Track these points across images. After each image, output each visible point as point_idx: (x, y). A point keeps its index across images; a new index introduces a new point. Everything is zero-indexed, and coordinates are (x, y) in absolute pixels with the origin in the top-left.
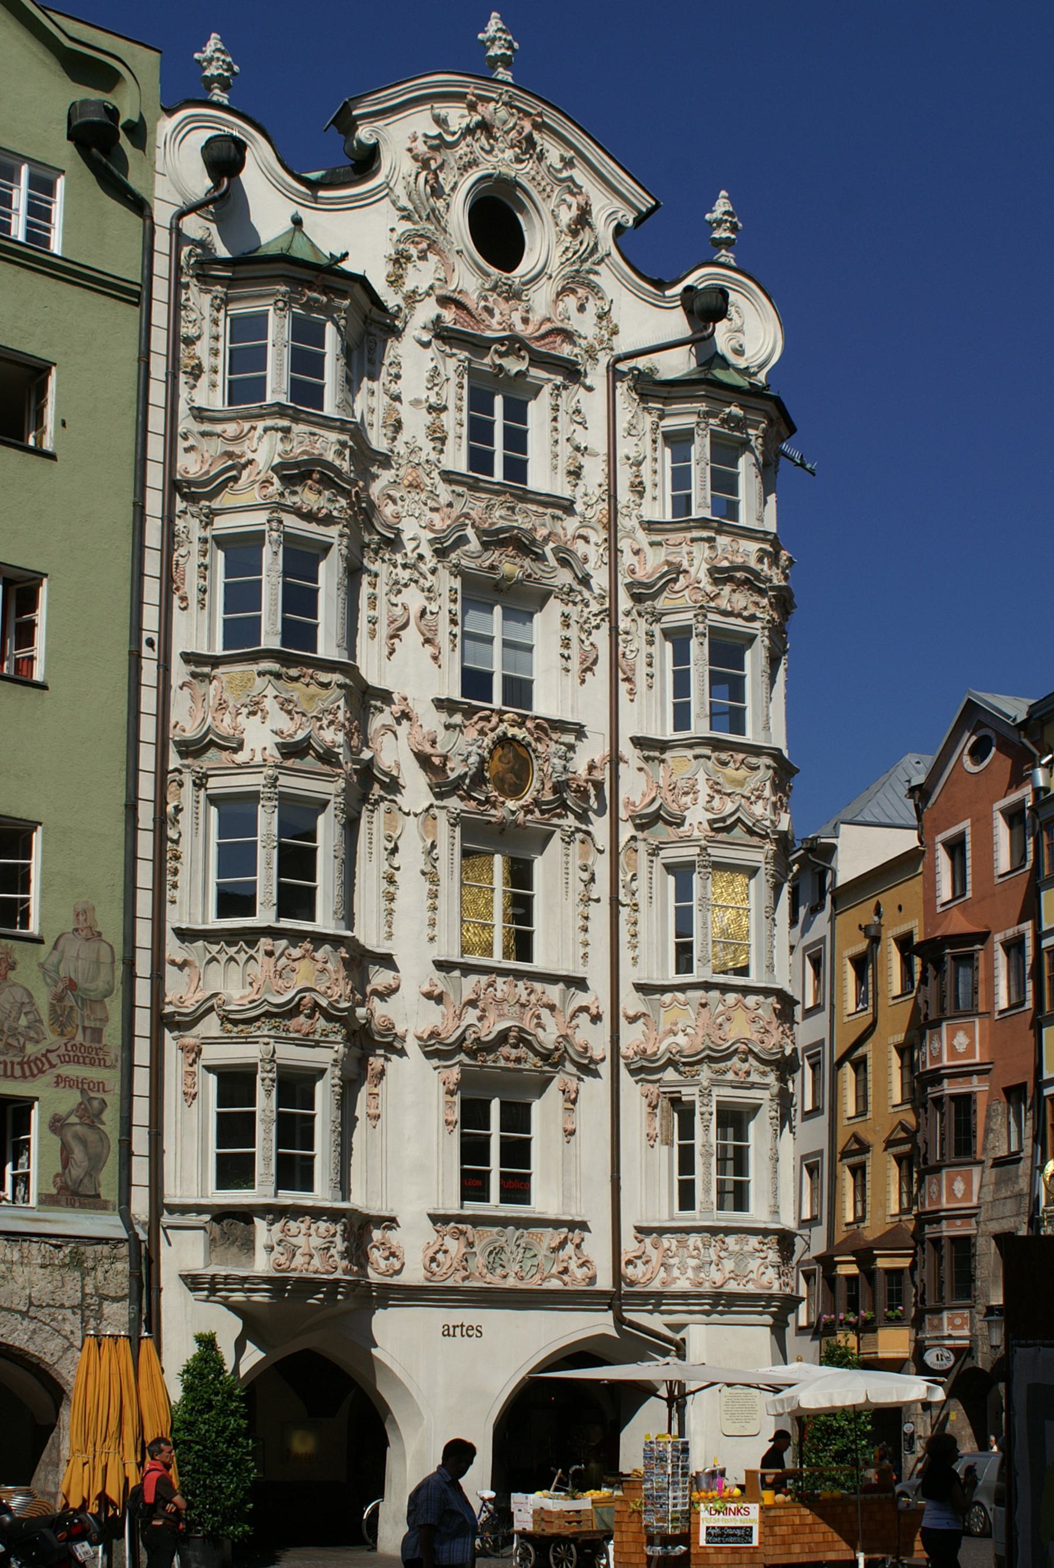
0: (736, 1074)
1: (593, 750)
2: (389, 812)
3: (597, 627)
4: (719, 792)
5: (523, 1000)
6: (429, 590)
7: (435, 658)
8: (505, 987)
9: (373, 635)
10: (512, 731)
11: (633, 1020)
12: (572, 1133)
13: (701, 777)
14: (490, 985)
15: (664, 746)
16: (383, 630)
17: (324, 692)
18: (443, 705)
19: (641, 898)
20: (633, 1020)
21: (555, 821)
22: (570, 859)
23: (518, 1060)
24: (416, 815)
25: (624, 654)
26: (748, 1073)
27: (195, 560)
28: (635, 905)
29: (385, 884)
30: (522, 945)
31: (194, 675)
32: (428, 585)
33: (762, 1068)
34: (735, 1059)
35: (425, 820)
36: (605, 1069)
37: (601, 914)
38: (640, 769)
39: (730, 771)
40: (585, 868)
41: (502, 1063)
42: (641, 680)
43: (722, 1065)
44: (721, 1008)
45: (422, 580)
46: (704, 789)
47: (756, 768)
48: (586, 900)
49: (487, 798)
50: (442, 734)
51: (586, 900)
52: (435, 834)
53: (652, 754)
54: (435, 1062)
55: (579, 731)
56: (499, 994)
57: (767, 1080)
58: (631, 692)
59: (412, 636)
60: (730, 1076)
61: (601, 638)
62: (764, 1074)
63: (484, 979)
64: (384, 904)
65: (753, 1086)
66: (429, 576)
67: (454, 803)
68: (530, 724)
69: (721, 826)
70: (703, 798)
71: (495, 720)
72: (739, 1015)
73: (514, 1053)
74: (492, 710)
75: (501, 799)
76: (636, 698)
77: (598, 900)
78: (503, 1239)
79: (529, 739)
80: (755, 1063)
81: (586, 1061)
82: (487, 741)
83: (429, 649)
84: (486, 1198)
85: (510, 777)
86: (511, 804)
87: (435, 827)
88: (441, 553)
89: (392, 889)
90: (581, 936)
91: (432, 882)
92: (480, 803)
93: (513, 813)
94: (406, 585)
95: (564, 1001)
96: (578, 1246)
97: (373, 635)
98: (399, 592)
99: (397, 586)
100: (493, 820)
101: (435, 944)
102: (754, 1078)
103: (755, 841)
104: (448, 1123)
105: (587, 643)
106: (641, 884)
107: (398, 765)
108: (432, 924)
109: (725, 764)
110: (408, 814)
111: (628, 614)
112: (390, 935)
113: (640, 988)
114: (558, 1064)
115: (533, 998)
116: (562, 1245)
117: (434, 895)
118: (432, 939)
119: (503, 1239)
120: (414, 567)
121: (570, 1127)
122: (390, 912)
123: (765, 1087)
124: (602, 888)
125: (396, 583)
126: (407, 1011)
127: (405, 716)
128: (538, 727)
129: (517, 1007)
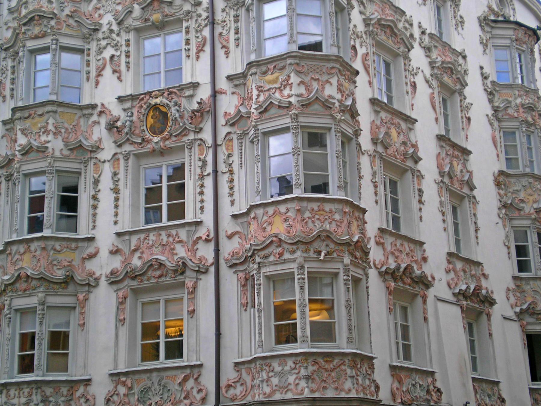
0: (274, 256)
1: (204, 93)
2: (95, 164)
3: (206, 25)
4: (262, 91)
5: (164, 242)
6: (116, 45)
7: (119, 78)
8: (154, 238)
9: (88, 79)
10: (153, 101)
11: (230, 237)
12: (194, 311)
13: (254, 85)
14: (145, 239)
15: (244, 75)
16: (93, 74)
17: (41, 119)
18: (121, 99)
19: (235, 167)
20: (230, 237)
21: (185, 139)
22: (192, 157)
23: (160, 277)
24: (109, 161)
25: (221, 34)
26: (281, 255)
27: (10, 76)
28: (231, 171)
29: (92, 202)
30: (177, 211)
31: (7, 130)
32: (115, 42)
33: (291, 247)
34: (273, 247)
35: (114, 162)
36: (212, 269)
37: (209, 182)
38: (233, 93)
39: (269, 77)
40: (200, 159)
41: (154, 280)
42: (232, 44)
43: (266, 252)
44: (265, 218)
45: (113, 42)
46: (255, 92)
47: (283, 68)
48: (202, 177)
49: (143, 140)
50: (123, 116)
51: (202, 177)
52: (119, 168)
53: (238, 83)
54: (115, 287)
55: (195, 86)
56: (151, 243)
57: (295, 256)
58: (227, 54)
59: (108, 71)
60: (272, 258)
61: (206, 32)
62: (292, 252)
63: (142, 236)
64: (92, 211)
65: (285, 261)
66: (118, 39)
67: (127, 148)
68: (166, 95)
69: (264, 111)
70: (254, 97)
71: (147, 97)
72: (278, 220)
73: (158, 273)
74: (145, 94)
75: (151, 137)
76: (231, 55)
77: (209, 174)
78: (151, 382)
79: (165, 101)
80: (286, 246)
81: (197, 269)
82: (143, 111)
83: (117, 74)
84: (157, 358)
85: (158, 125)
86: (156, 139)
87: (119, 164)
88: (120, 23)
89: (96, 202)
90: (199, 198)
91: (116, 193)
92: (141, 144)
93: (157, 143)
94: (105, 48)
95: (188, 237)
96: (196, 379)
97: (88, 79)
98: (102, 52)
99: (100, 51)
100: (148, 150)
101: (117, 225)
102: (287, 256)
103: (284, 111)
104: (121, 321)
105: (200, 37)
106: (235, 158)
107: (100, 140)
108: (116, 215)
109: (265, 73)
110: (104, 162)
111: (223, 10)
112: (94, 227)
113: (235, 217)
114: (183, 273)
115: (171, 239)
116: (186, 379)
117: (117, 199)
118: (116, 223)
119: (151, 382)
120: (107, 38)
121: (191, 308)
122: (95, 215)
123: (294, 260)
124: (209, 169)
125: (100, 49)
126: (104, 264)
127: (101, 113)
128: (171, 93)
129: (160, 248)
